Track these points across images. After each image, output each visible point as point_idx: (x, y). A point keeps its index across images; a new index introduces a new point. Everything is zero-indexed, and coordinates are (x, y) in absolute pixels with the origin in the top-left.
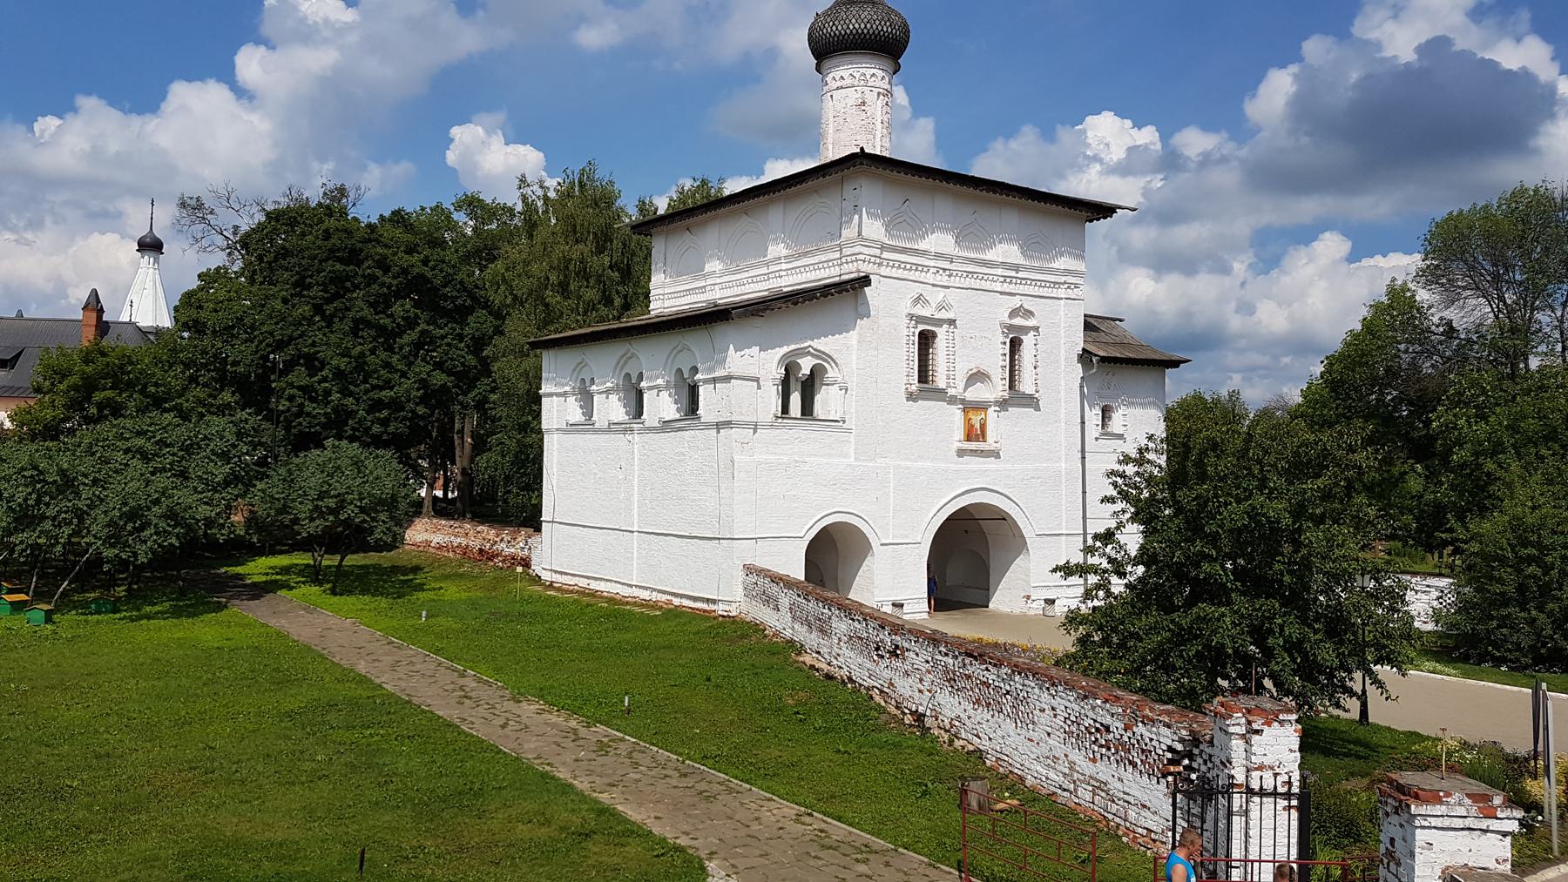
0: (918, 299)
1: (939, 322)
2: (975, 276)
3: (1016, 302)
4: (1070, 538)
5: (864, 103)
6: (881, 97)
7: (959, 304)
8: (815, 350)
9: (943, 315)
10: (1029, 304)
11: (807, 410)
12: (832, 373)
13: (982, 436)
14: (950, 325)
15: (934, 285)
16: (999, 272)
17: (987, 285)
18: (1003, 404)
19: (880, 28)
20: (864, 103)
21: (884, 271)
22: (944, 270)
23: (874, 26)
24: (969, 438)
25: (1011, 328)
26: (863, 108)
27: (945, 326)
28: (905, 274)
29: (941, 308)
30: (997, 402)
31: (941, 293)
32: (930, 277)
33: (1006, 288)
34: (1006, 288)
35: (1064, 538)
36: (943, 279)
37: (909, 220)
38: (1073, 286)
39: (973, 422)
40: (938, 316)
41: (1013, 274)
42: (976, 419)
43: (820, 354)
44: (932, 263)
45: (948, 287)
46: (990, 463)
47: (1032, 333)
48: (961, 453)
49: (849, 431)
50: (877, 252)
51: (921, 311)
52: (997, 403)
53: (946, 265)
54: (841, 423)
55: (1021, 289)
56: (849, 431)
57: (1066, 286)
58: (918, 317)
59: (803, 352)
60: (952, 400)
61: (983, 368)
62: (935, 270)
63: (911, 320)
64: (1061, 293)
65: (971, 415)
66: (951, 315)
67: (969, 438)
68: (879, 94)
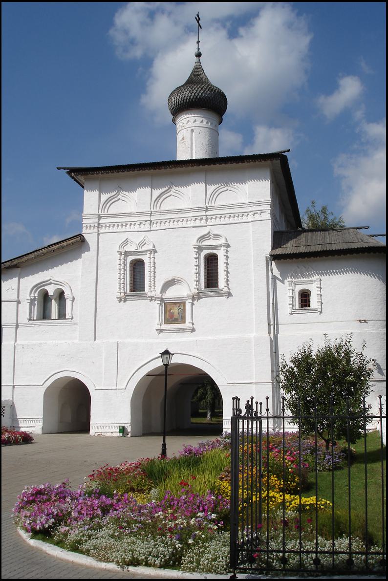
0: (126, 242)
1: (143, 252)
2: (172, 220)
3: (205, 231)
4: (260, 386)
7: (153, 238)
9: (145, 248)
10: (215, 230)
11: (62, 315)
12: (67, 293)
14: (151, 253)
15: (138, 232)
16: (191, 214)
17: (184, 224)
18: (196, 297)
19: (183, 96)
21: (89, 231)
22: (146, 221)
23: (181, 96)
26: (183, 141)
27: (148, 254)
28: (120, 229)
29: (142, 243)
30: (188, 297)
32: (137, 228)
33: (198, 223)
34: (198, 223)
35: (254, 386)
36: (147, 227)
37: (123, 198)
38: (259, 212)
41: (203, 213)
42: (175, 310)
43: (57, 283)
45: (150, 231)
46: (188, 337)
47: (223, 248)
49: (76, 324)
51: (128, 248)
53: (148, 218)
54: (70, 320)
55: (213, 222)
56: (76, 324)
57: (253, 213)
59: (48, 283)
60: (152, 299)
62: (139, 223)
63: (121, 254)
64: (250, 218)
66: (151, 248)
67: (167, 321)
68: (192, 131)
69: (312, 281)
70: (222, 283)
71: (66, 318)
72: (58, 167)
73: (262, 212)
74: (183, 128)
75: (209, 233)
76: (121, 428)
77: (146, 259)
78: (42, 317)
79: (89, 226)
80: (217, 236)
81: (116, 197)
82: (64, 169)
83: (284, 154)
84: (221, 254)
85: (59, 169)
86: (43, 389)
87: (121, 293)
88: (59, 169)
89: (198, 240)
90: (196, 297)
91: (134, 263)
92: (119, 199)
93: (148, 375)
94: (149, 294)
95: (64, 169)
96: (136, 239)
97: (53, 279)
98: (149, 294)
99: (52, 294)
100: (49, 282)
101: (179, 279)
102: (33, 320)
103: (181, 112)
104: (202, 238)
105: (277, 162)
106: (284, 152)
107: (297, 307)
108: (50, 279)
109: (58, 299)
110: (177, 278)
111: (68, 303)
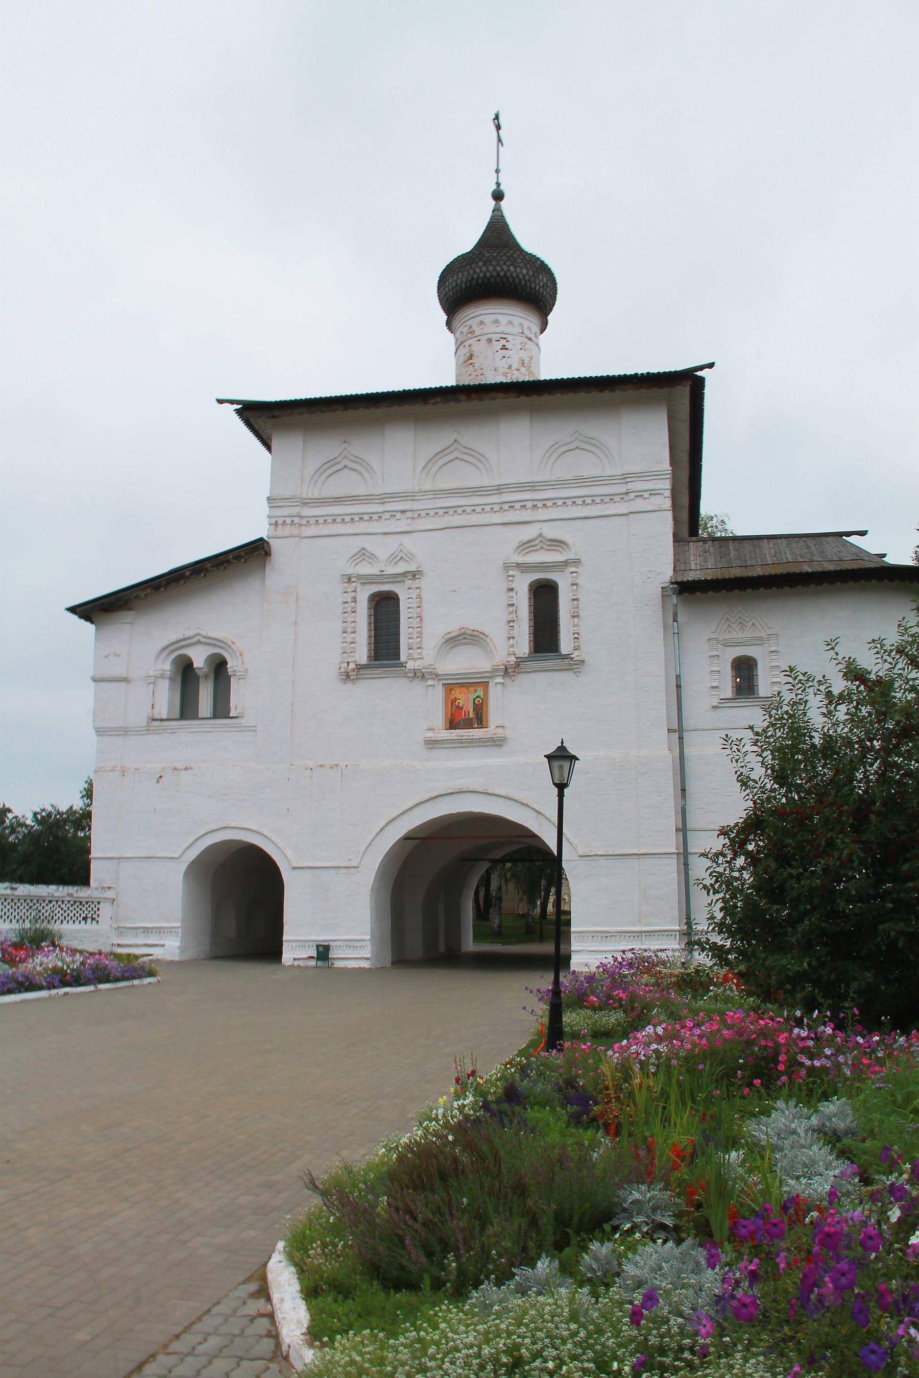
3: (529, 532)
5: (471, 357)
6: (495, 343)
8: (206, 637)
9: (401, 568)
10: (551, 532)
11: (221, 710)
13: (479, 718)
20: (471, 357)
21: (280, 532)
24: (452, 724)
25: (524, 568)
26: (470, 362)
31: (393, 544)
36: (403, 525)
38: (646, 495)
39: (461, 703)
40: (391, 570)
42: (466, 700)
43: (211, 642)
44: (380, 508)
48: (432, 744)
49: (252, 729)
50: (294, 511)
51: (366, 569)
52: (493, 672)
57: (632, 496)
58: (359, 577)
61: (472, 623)
65: (457, 693)
66: (413, 568)
67: (452, 724)
69: (760, 638)
70: (565, 645)
71: (231, 715)
72: (220, 398)
73: (653, 493)
74: (470, 335)
75: (541, 535)
76: (321, 949)
77: (400, 590)
78: (178, 716)
79: (280, 521)
80: (558, 544)
81: (339, 463)
82: (232, 402)
83: (699, 373)
84: (563, 583)
85: (220, 402)
86: (183, 867)
87: (348, 663)
88: (220, 402)
89: (519, 547)
90: (509, 671)
91: (377, 599)
92: (346, 466)
93: (407, 838)
94: (410, 665)
95: (232, 402)
96: (382, 549)
97: (204, 633)
98: (410, 665)
99: (202, 666)
100: (195, 640)
101: (475, 633)
102: (161, 720)
103: (455, 314)
104: (527, 546)
105: (684, 392)
106: (701, 368)
107: (728, 692)
108: (198, 634)
109: (212, 676)
110: (469, 632)
111: (236, 687)
